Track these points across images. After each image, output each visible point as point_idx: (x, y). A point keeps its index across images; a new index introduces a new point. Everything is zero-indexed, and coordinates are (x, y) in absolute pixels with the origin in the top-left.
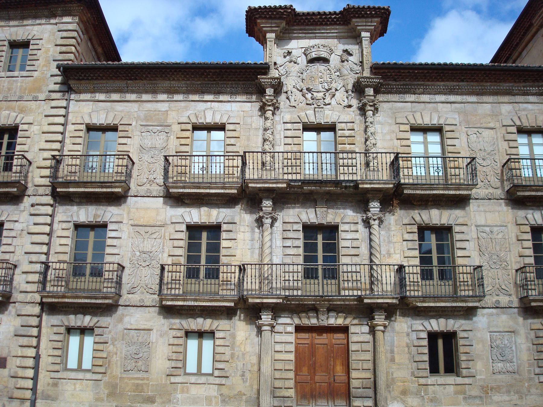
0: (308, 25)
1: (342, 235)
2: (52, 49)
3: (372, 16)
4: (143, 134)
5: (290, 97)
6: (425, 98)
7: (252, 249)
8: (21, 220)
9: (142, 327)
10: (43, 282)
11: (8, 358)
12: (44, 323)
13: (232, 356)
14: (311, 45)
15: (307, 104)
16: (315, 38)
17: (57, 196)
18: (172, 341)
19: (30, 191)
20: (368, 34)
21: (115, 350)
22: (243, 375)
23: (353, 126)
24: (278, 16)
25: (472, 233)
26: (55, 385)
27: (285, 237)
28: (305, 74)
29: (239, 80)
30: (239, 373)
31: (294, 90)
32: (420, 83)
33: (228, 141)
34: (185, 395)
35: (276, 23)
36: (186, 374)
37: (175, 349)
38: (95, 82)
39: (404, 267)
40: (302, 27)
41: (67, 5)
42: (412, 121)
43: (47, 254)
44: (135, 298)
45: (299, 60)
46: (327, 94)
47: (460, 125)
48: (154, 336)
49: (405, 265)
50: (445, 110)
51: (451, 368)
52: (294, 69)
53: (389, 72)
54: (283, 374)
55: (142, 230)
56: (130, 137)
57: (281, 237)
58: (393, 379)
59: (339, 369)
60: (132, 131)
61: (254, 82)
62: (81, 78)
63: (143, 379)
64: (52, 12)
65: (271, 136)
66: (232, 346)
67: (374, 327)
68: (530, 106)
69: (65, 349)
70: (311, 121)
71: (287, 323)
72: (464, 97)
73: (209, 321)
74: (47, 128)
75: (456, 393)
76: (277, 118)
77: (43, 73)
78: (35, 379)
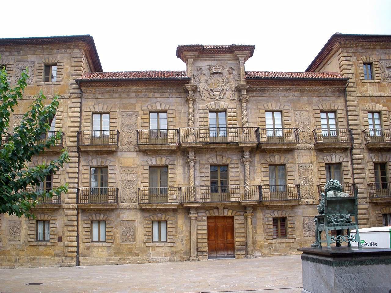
0: (210, 53)
2: (69, 69)
3: (245, 50)
4: (123, 116)
5: (202, 94)
6: (273, 94)
7: (184, 178)
9: (130, 219)
10: (77, 198)
11: (63, 237)
12: (80, 219)
13: (176, 232)
14: (212, 65)
15: (211, 98)
16: (214, 60)
17: (80, 152)
18: (145, 226)
21: (117, 231)
22: (182, 242)
23: (235, 111)
24: (194, 50)
26: (88, 249)
27: (201, 171)
28: (209, 81)
29: (174, 86)
30: (180, 241)
31: (204, 91)
32: (270, 86)
33: (169, 120)
34: (154, 252)
35: (193, 53)
36: (153, 242)
37: (147, 230)
38: (96, 88)
39: (262, 186)
43: (78, 183)
44: (125, 205)
46: (221, 93)
47: (291, 109)
48: (136, 224)
49: (262, 185)
51: (284, 235)
52: (204, 78)
53: (254, 81)
54: (202, 240)
55: (126, 169)
56: (116, 119)
57: (199, 171)
58: (256, 241)
59: (229, 237)
60: (117, 115)
61: (182, 87)
63: (132, 245)
65: (192, 117)
66: (176, 227)
67: (246, 216)
68: (328, 98)
70: (213, 108)
72: (294, 93)
73: (164, 216)
74: (71, 114)
75: (286, 247)
76: (195, 106)
77: (66, 83)
78: (78, 247)
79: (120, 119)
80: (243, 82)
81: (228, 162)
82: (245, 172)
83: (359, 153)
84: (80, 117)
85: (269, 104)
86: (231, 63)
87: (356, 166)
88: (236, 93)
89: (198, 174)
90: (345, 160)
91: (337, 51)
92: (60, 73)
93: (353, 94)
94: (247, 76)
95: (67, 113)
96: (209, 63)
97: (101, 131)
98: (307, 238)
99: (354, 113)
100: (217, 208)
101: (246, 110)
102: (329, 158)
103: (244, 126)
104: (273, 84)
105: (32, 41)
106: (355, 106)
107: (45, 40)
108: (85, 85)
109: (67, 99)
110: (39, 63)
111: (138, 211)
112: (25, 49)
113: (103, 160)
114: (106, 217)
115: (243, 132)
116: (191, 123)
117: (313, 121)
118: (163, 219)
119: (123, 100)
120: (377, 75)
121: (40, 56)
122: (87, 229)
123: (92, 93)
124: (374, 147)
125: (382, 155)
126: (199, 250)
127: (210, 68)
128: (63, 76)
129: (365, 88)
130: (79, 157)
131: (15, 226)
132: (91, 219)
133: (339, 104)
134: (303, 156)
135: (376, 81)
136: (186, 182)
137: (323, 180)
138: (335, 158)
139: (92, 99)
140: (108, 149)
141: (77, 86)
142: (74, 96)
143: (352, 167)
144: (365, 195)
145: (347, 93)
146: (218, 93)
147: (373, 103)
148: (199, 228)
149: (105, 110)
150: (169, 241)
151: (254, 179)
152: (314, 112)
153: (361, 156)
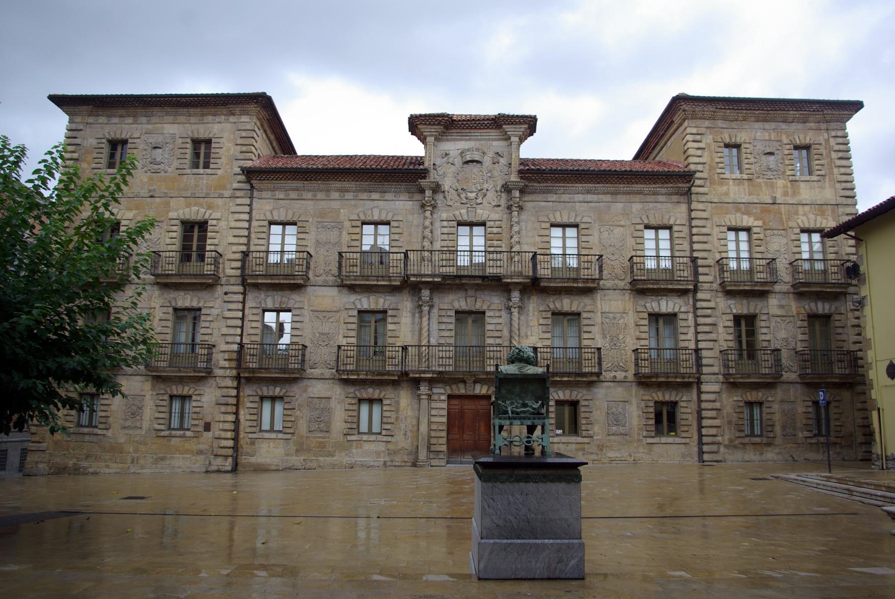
1: (488, 320)
3: (521, 123)
6: (565, 197)
7: (412, 331)
8: (217, 306)
13: (397, 419)
14: (466, 147)
18: (347, 407)
19: (223, 281)
20: (517, 139)
22: (405, 434)
25: (598, 318)
26: (253, 444)
30: (402, 433)
34: (359, 450)
36: (359, 433)
37: (350, 413)
40: (459, 131)
42: (553, 220)
43: (241, 335)
44: (316, 372)
45: (456, 163)
48: (333, 403)
50: (582, 209)
55: (321, 315)
59: (482, 429)
63: (325, 438)
66: (397, 411)
68: (658, 205)
69: (260, 414)
71: (441, 392)
72: (600, 196)
73: (377, 391)
74: (233, 224)
76: (435, 216)
79: (313, 233)
80: (514, 178)
81: (485, 307)
82: (511, 324)
83: (709, 298)
84: (249, 229)
85: (558, 214)
86: (498, 145)
87: (701, 320)
88: (503, 195)
89: (435, 326)
90: (683, 309)
91: (681, 124)
93: (703, 199)
94: (522, 167)
96: (462, 145)
97: (282, 252)
98: (612, 437)
99: (704, 231)
100: (463, 381)
101: (518, 223)
102: (655, 304)
103: (514, 250)
104: (564, 180)
106: (706, 219)
111: (337, 382)
113: (283, 299)
114: (284, 391)
115: (512, 259)
116: (427, 244)
117: (630, 242)
118: (376, 396)
119: (320, 202)
120: (747, 166)
122: (252, 411)
123: (268, 190)
124: (734, 288)
125: (749, 303)
126: (433, 448)
127: (462, 153)
129: (725, 188)
130: (244, 294)
131: (134, 405)
132: (260, 393)
133: (677, 213)
134: (610, 300)
135: (745, 177)
136: (416, 338)
137: (643, 342)
138: (666, 305)
140: (292, 282)
141: (243, 178)
142: (238, 193)
143: (696, 321)
144: (715, 369)
145: (693, 196)
146: (473, 195)
147: (738, 215)
148: (433, 412)
149: (289, 218)
150: (384, 432)
151: (527, 337)
152: (633, 229)
153: (712, 304)
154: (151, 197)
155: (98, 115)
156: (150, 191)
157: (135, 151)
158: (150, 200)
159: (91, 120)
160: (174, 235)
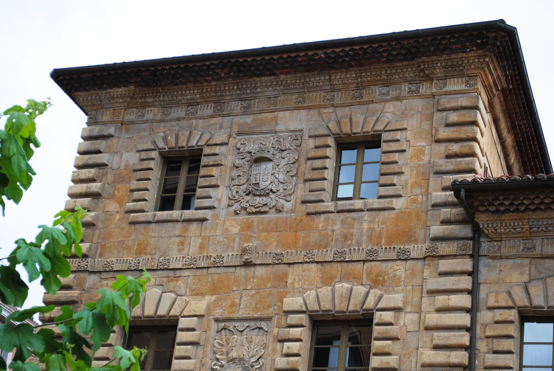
2: (427, 151)
38: (534, 215)
41: (454, 56)
62: (502, 209)
64: (423, 70)
74: (433, 319)
92: (394, 168)
95: (417, 315)
105: (295, 59)
107: (337, 50)
108: (491, 205)
109: (420, 263)
110: (316, 136)
112: (269, 92)
121: (320, 114)
128: (403, 177)
139: (518, 261)
142: (444, 248)
154: (247, 264)
155: (144, 106)
156: (244, 251)
157: (215, 171)
158: (241, 272)
159: (131, 115)
160: (295, 347)
